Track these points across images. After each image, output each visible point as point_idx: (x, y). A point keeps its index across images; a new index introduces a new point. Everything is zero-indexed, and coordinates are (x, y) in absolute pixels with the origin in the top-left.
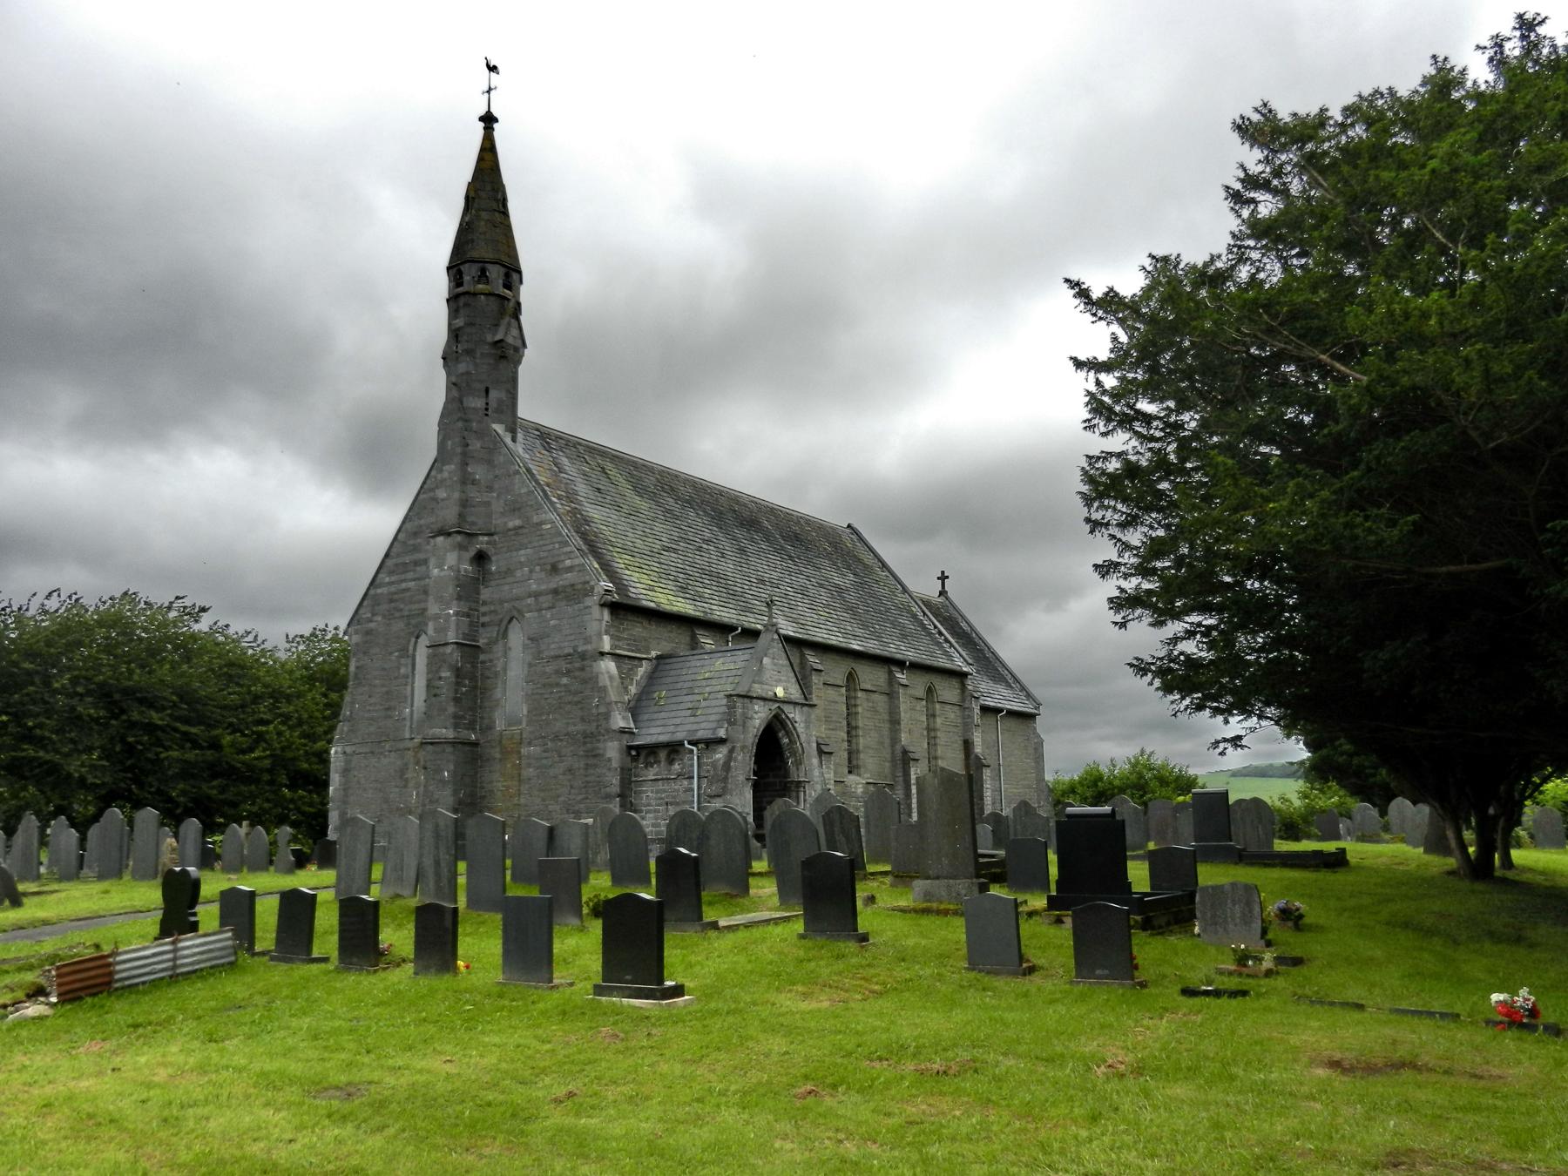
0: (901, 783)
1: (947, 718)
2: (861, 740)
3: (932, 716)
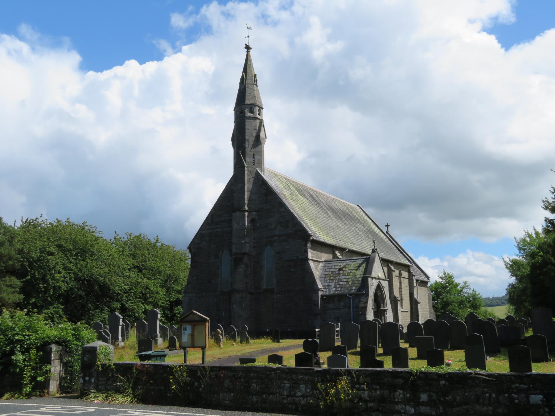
1: (405, 283)
3: (400, 283)
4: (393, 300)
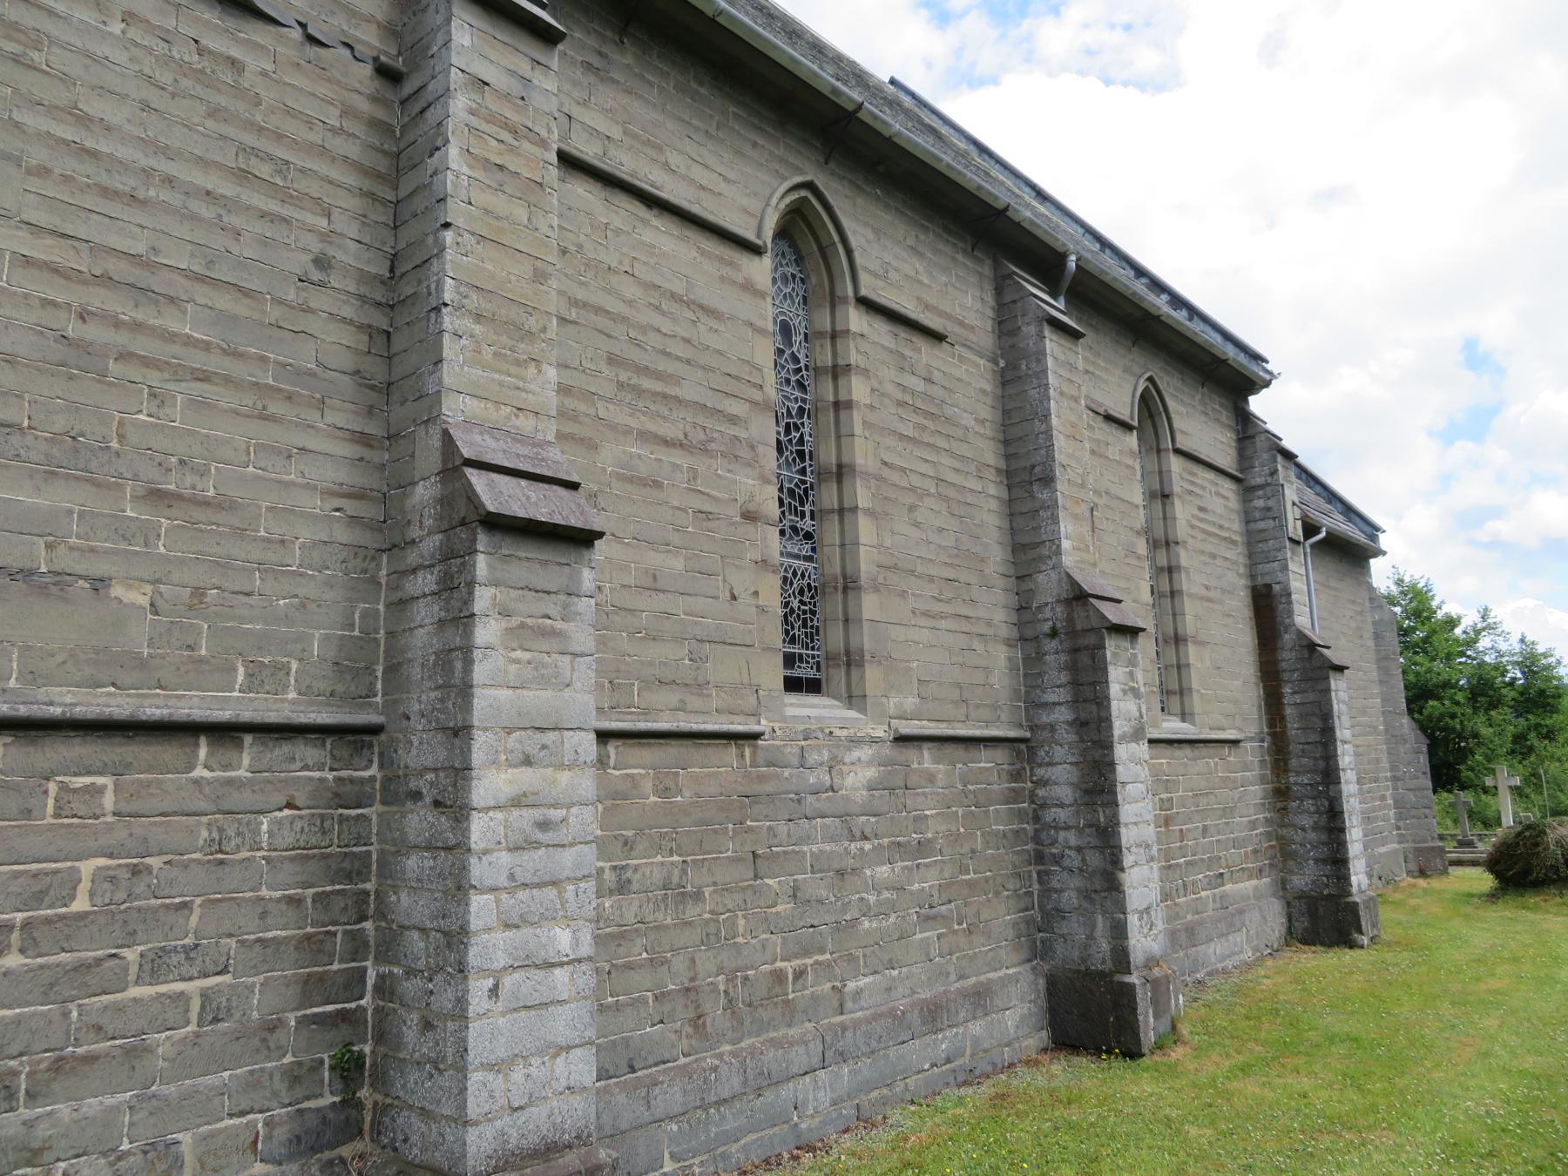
0: (1066, 735)
2: (865, 530)
3: (1161, 495)
4: (1054, 633)
